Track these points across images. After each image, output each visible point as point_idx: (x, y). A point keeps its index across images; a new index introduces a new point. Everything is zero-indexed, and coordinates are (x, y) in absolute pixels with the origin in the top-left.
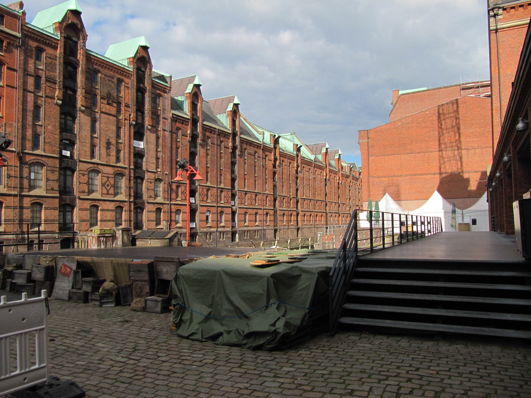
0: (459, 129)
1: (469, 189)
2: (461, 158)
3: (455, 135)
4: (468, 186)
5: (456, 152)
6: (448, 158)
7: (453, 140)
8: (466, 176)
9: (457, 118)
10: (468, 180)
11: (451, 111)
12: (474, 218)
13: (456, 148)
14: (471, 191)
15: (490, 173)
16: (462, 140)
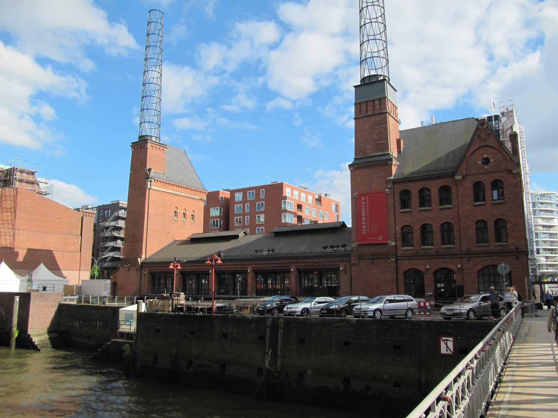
0: (15, 212)
1: (17, 260)
2: (14, 235)
3: (12, 216)
4: (16, 259)
5: (11, 230)
6: (4, 232)
7: (10, 219)
8: (16, 250)
9: (15, 203)
10: (17, 254)
11: (12, 194)
12: (45, 285)
13: (11, 226)
14: (19, 262)
15: (142, 263)
16: (18, 221)
